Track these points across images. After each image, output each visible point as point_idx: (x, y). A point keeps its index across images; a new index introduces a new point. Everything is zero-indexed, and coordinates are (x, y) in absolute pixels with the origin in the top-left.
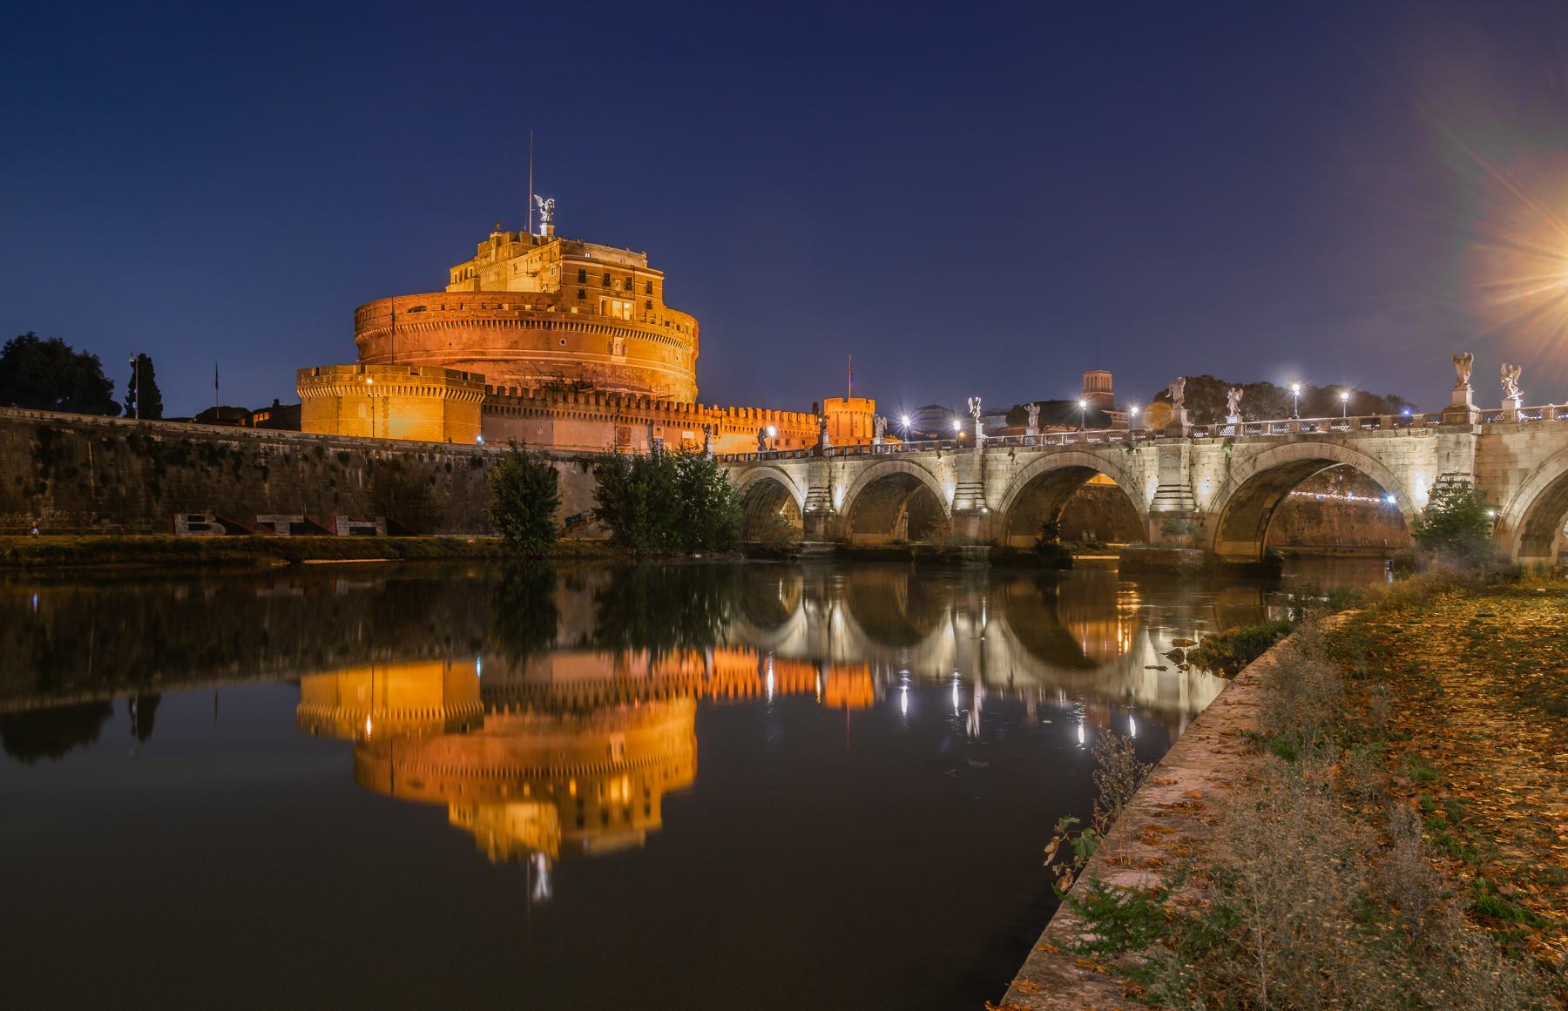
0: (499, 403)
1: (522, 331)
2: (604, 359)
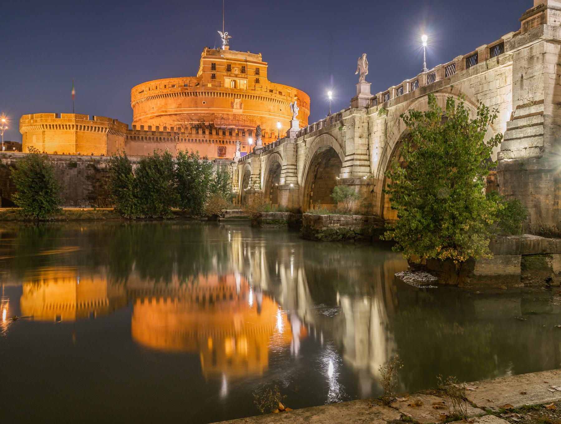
0: (140, 135)
1: (184, 98)
2: (229, 111)
